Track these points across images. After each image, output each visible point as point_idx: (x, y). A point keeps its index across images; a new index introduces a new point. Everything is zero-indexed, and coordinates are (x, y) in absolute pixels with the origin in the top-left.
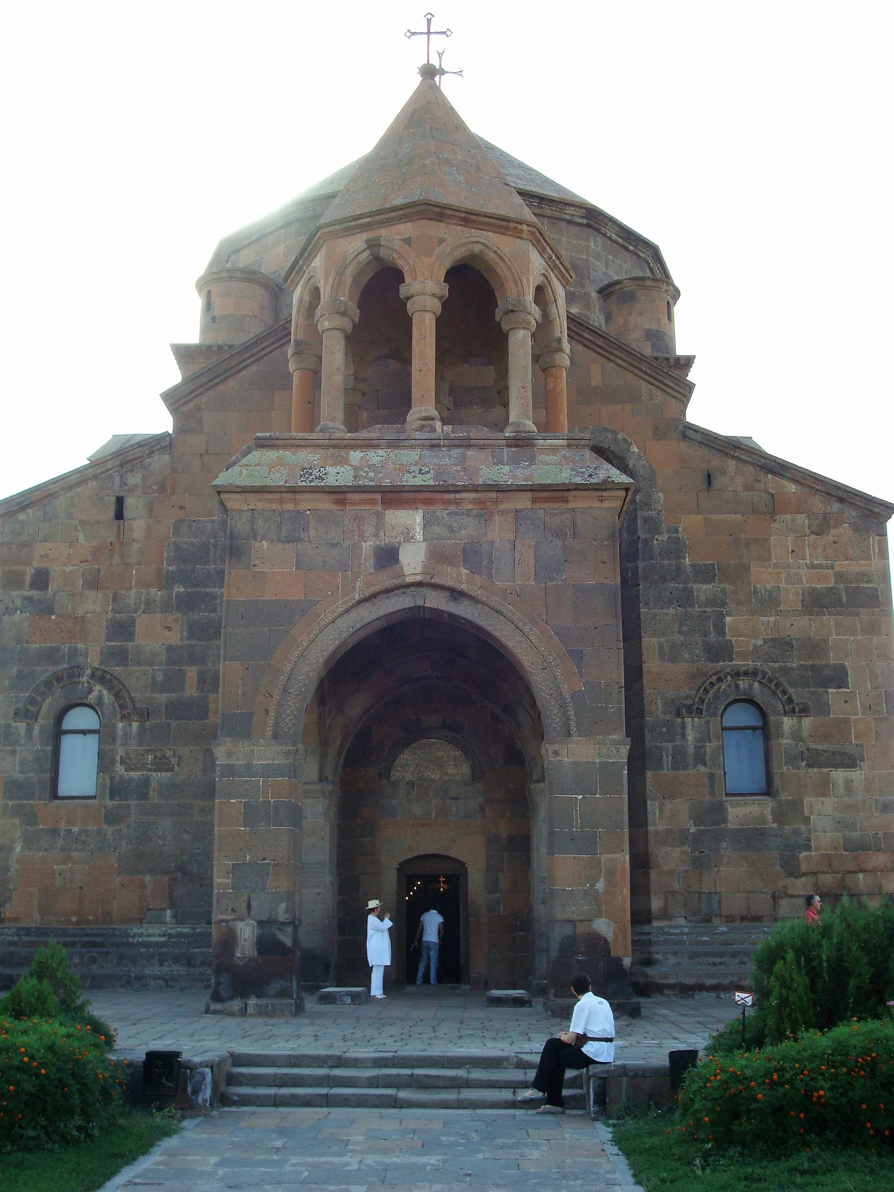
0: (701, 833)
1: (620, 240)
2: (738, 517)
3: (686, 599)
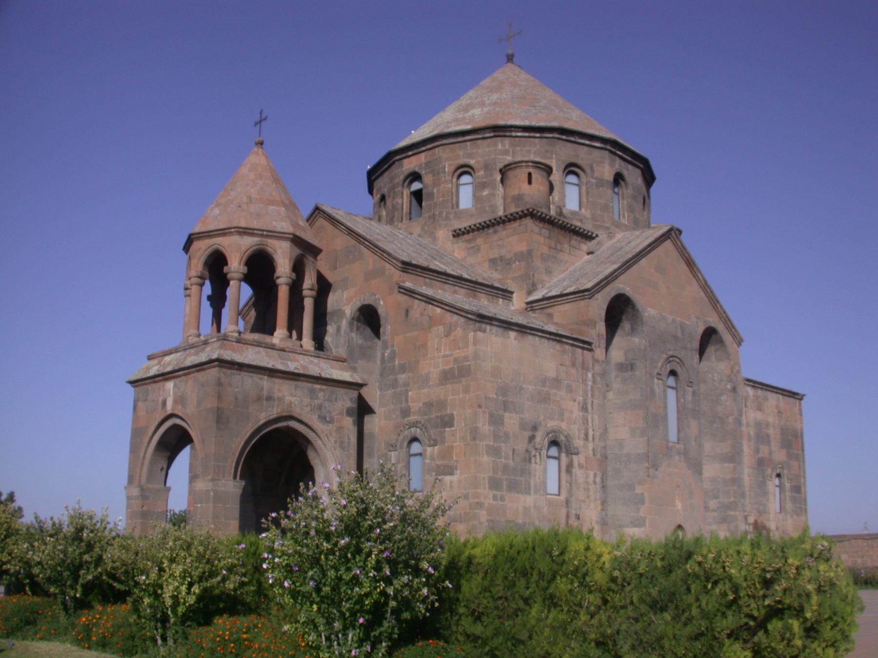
2: (416, 333)
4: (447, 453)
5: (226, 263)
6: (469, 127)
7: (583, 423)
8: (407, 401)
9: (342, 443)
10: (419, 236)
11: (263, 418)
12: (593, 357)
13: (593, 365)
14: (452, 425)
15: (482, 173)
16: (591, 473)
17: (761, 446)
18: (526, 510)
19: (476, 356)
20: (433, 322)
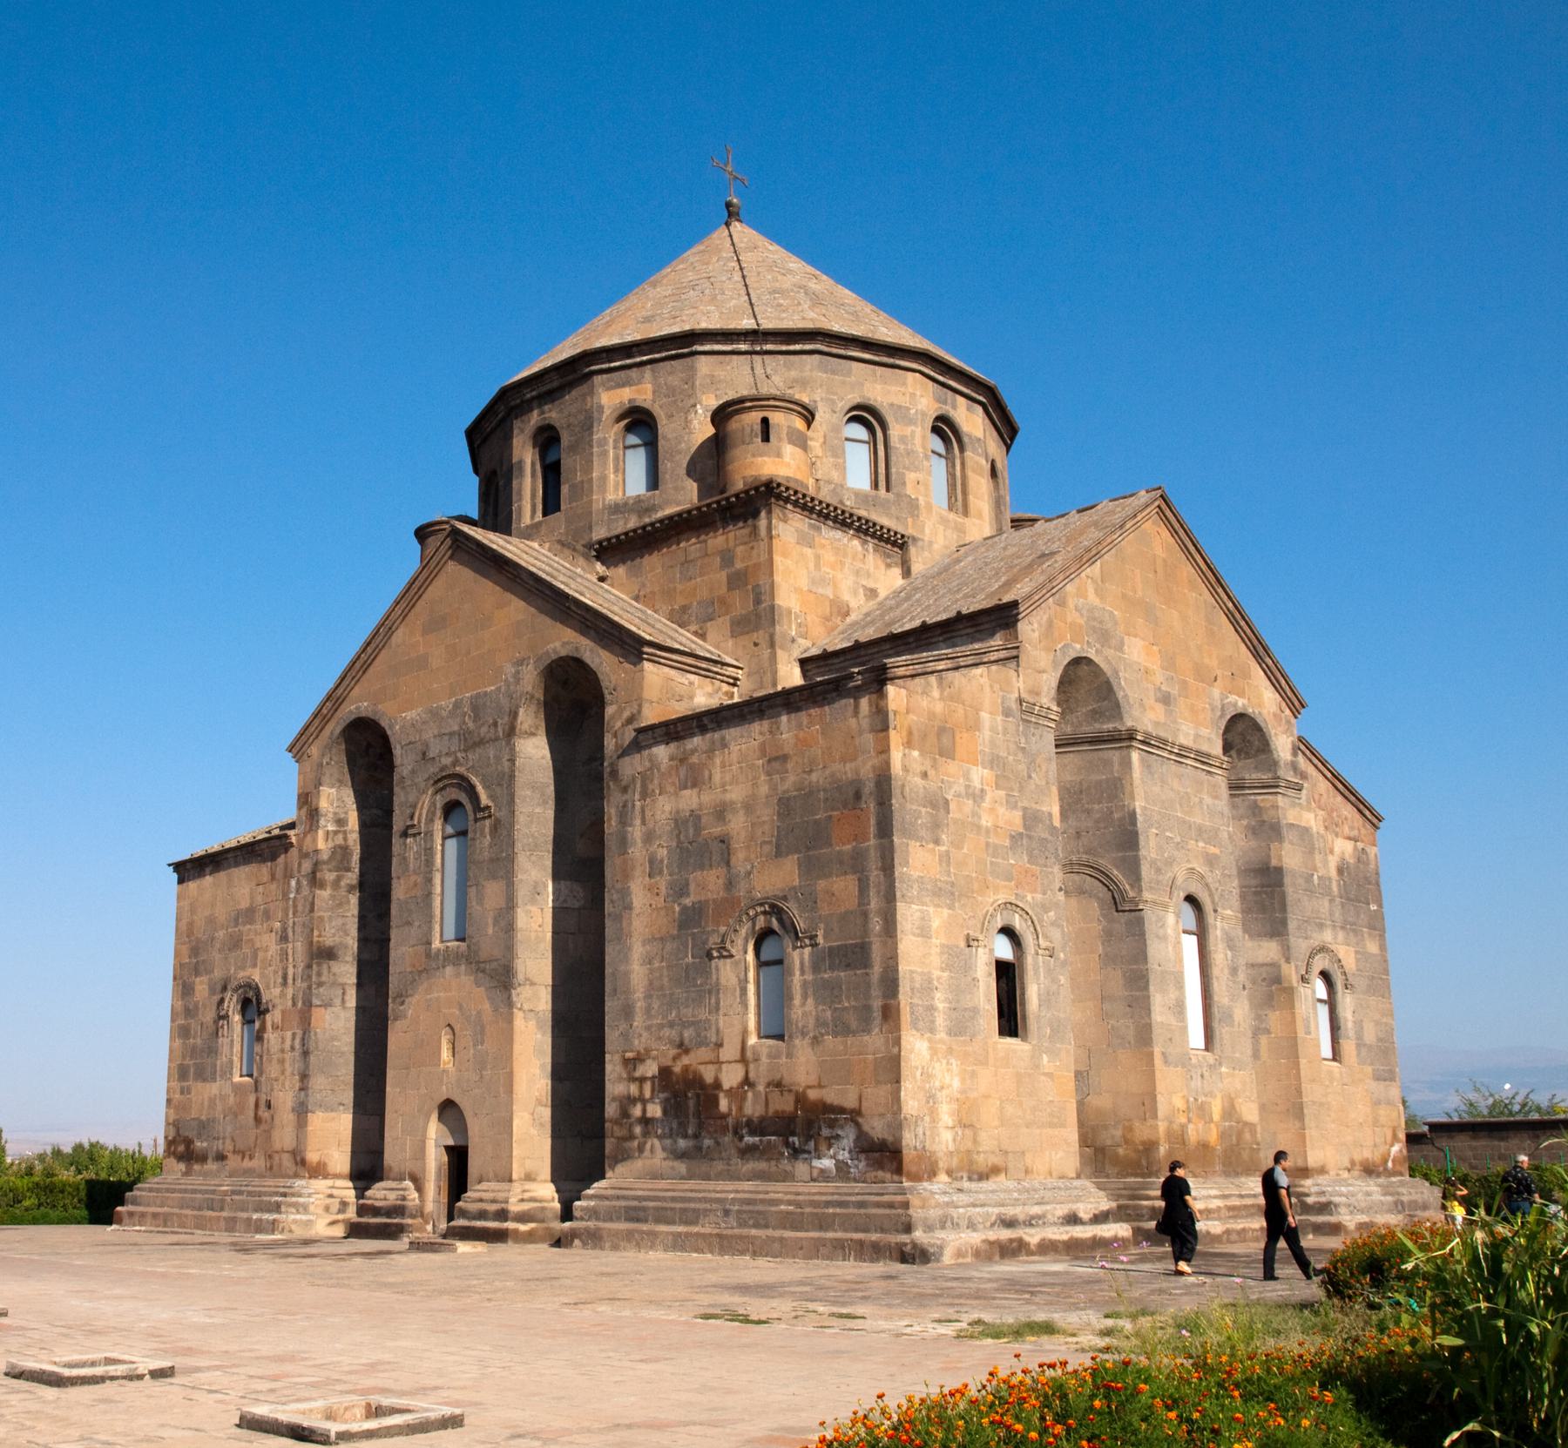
13: (300, 865)
16: (289, 1034)
17: (696, 877)
18: (212, 1101)
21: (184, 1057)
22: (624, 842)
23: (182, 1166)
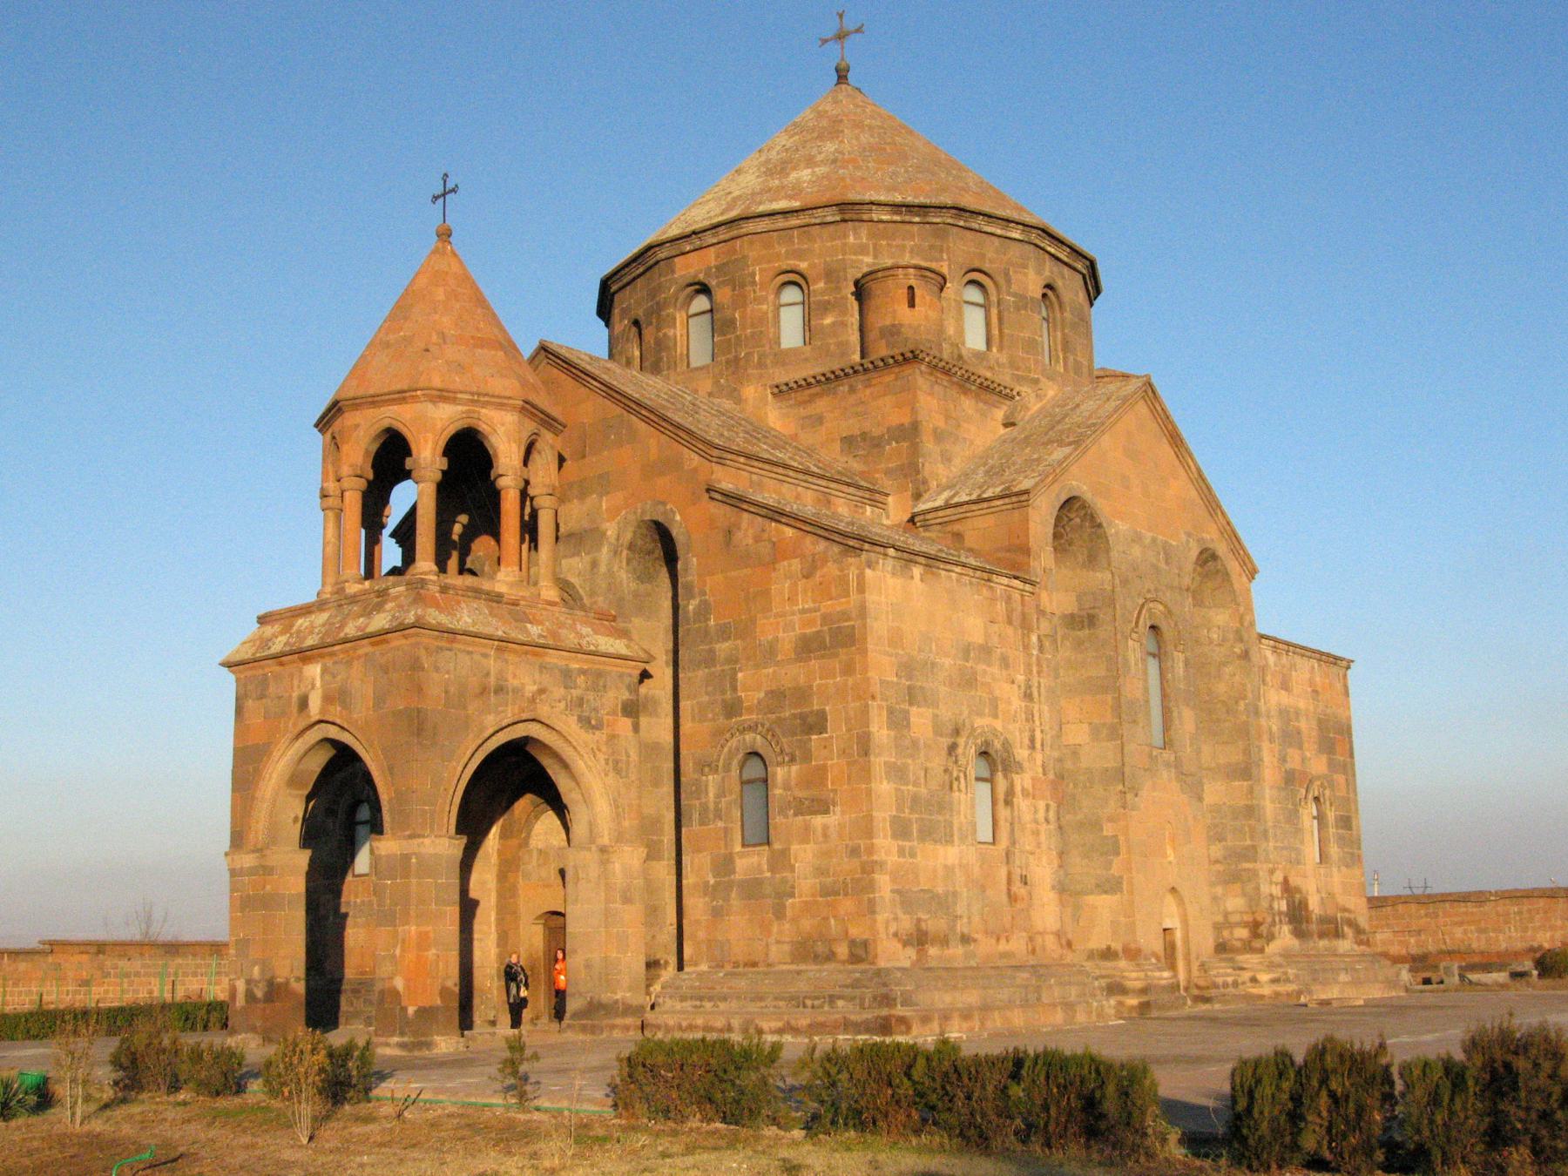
0: (717, 884)
1: (897, 218)
2: (748, 571)
3: (710, 659)
4: (817, 777)
5: (409, 453)
6: (796, 204)
7: (1027, 720)
8: (734, 689)
9: (617, 762)
10: (710, 394)
11: (491, 722)
12: (1038, 606)
14: (823, 730)
15: (821, 285)
16: (1041, 805)
17: (1290, 751)
19: (863, 612)
20: (780, 552)
21: (900, 809)
22: (1257, 713)
23: (911, 952)
